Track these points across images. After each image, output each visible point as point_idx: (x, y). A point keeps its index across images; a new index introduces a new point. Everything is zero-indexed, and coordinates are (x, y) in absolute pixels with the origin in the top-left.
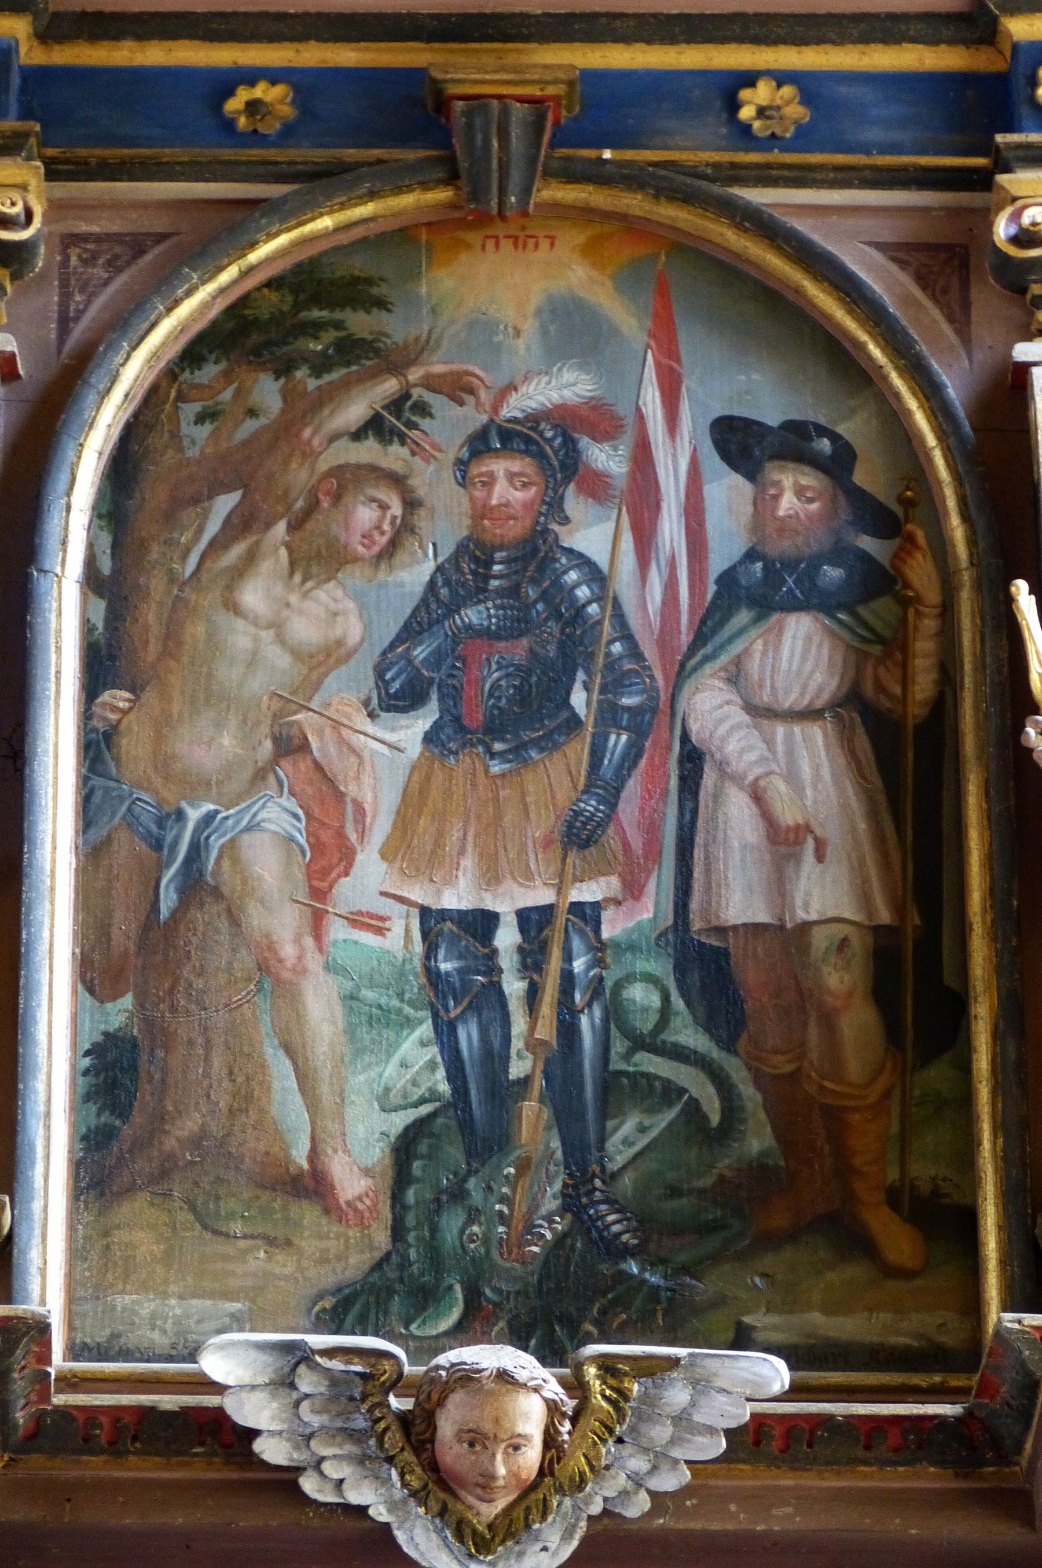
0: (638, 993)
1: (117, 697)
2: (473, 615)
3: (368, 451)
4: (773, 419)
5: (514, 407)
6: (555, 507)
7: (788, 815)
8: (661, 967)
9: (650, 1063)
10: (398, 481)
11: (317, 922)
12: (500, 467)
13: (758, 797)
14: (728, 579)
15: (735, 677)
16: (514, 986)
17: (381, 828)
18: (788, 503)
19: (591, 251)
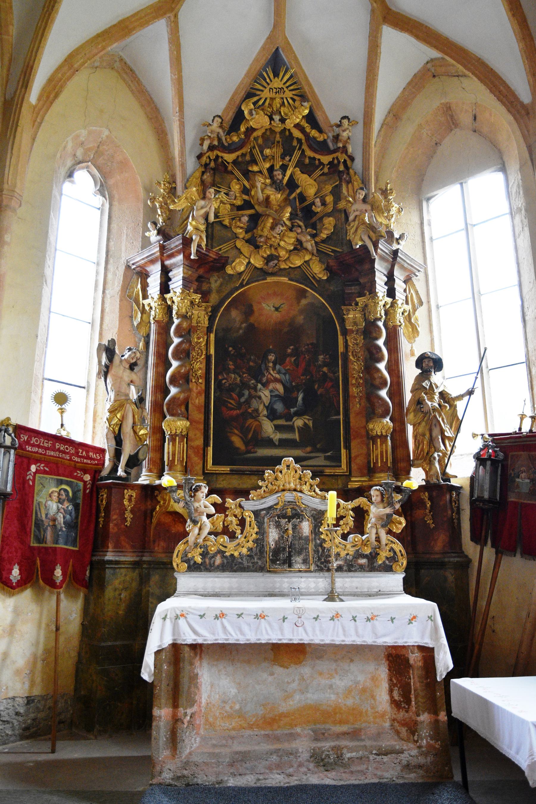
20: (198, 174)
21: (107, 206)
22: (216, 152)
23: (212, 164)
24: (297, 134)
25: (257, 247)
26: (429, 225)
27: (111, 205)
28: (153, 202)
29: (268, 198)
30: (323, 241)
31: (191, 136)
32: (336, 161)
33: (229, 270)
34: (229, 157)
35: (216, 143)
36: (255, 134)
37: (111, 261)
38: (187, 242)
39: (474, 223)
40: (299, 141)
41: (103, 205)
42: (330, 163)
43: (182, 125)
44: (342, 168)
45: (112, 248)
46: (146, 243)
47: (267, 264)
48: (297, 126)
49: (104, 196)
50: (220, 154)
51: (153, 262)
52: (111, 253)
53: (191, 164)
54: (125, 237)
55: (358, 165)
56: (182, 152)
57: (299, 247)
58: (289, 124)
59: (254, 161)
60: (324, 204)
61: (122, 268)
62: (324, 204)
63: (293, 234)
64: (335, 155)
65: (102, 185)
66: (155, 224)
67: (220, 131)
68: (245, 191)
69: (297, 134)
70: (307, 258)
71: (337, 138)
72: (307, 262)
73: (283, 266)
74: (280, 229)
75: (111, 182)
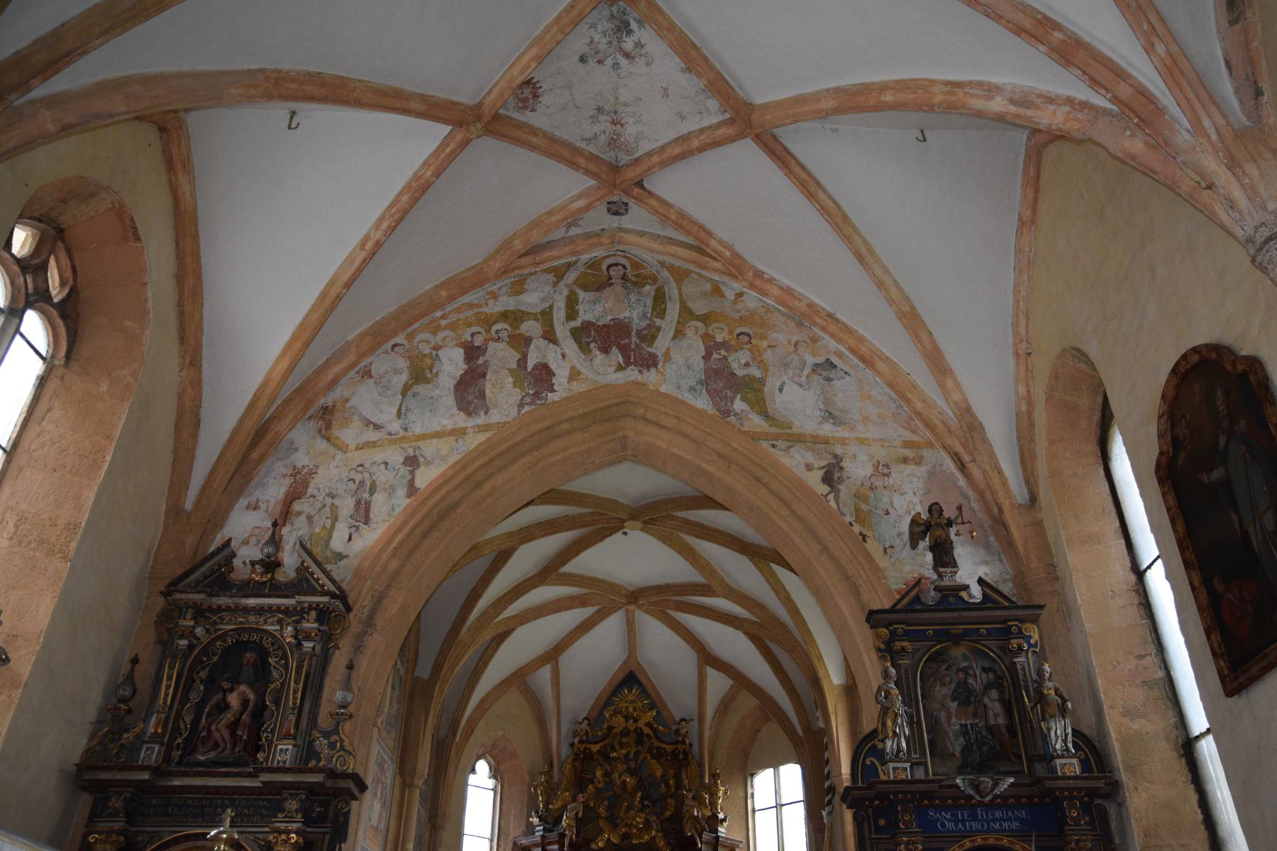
0: (984, 733)
1: (925, 701)
2: (960, 690)
3: (946, 672)
4: (987, 666)
5: (961, 666)
6: (966, 678)
7: (996, 712)
8: (985, 729)
9: (986, 740)
10: (950, 675)
11: (949, 726)
12: (960, 673)
13: (992, 710)
14: (986, 685)
15: (988, 696)
16: (971, 732)
17: (954, 714)
18: (990, 677)
19: (966, 648)
20: (570, 760)
21: (499, 788)
22: (584, 745)
23: (582, 756)
24: (647, 730)
25: (615, 826)
26: (753, 797)
27: (502, 787)
28: (535, 790)
29: (624, 782)
30: (667, 820)
31: (565, 727)
32: (677, 751)
33: (593, 846)
34: (595, 748)
35: (584, 738)
36: (614, 731)
37: (502, 838)
38: (562, 836)
39: (783, 803)
40: (648, 735)
41: (496, 787)
42: (673, 751)
43: (559, 723)
44: (681, 757)
45: (503, 826)
46: (530, 829)
47: (623, 840)
48: (648, 725)
49: (497, 780)
50: (588, 746)
51: (536, 845)
52: (501, 831)
53: (565, 750)
54: (512, 817)
55: (696, 749)
56: (559, 744)
57: (647, 824)
58: (641, 724)
59: (614, 749)
60: (667, 786)
61: (510, 845)
62: (667, 786)
63: (643, 815)
64: (676, 746)
65: (495, 770)
66: (537, 812)
67: (588, 728)
68: (607, 774)
69: (647, 730)
70: (654, 833)
71: (677, 732)
72: (654, 838)
73: (635, 842)
74: (632, 813)
75: (503, 768)
